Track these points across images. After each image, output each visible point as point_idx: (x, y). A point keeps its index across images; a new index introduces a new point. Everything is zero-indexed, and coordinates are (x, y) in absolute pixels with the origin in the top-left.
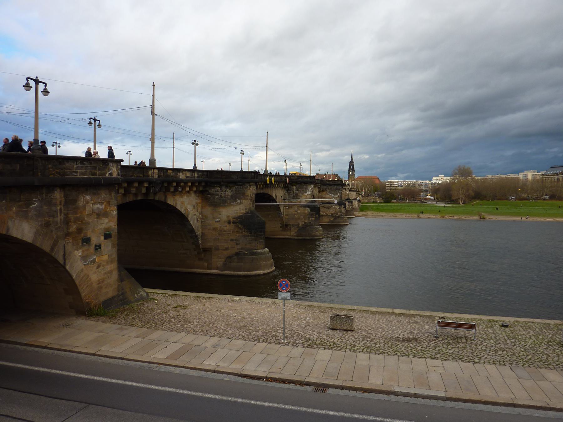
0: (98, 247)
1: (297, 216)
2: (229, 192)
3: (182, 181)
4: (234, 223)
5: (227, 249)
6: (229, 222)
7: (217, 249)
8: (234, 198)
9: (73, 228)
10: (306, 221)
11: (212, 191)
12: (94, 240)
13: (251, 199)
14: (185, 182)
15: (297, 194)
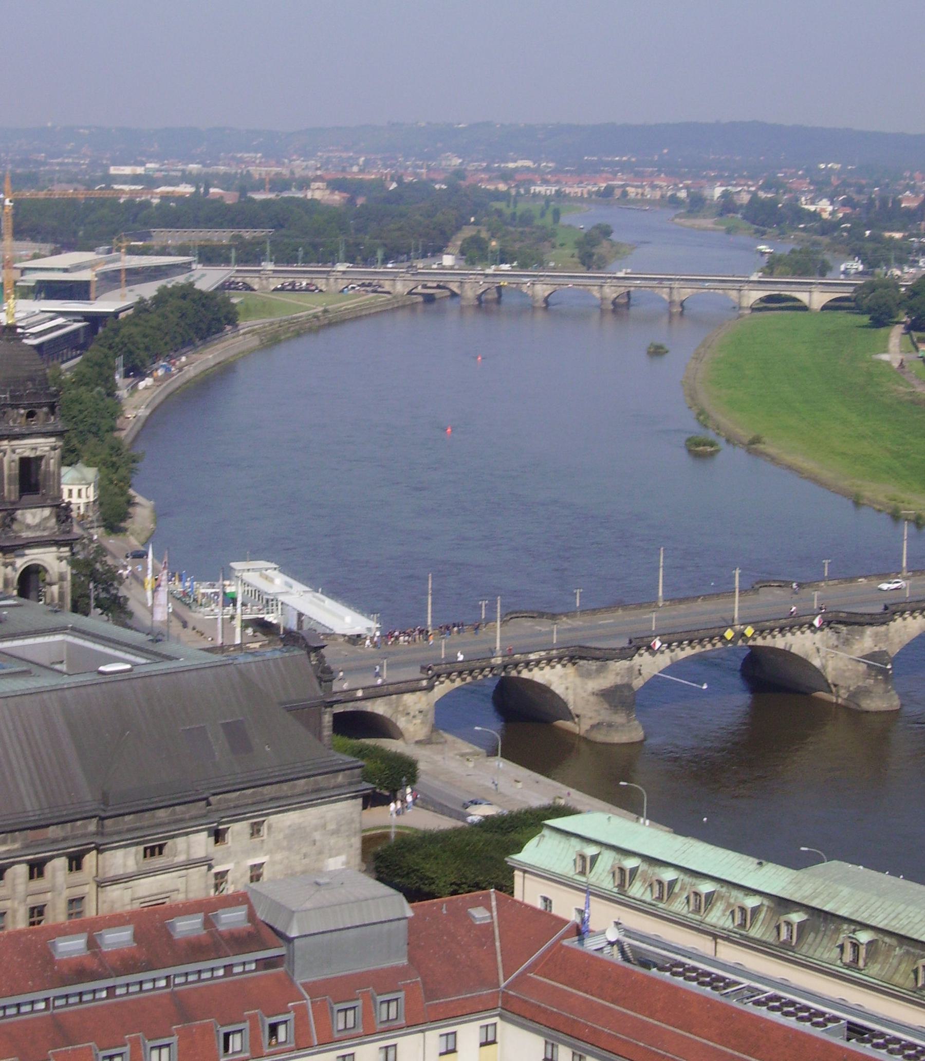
0: (414, 717)
1: (847, 674)
2: (593, 665)
3: (532, 661)
4: (597, 695)
5: (591, 718)
6: (593, 693)
7: (585, 716)
8: (599, 671)
9: (401, 708)
10: (860, 684)
11: (582, 662)
12: (412, 714)
13: (617, 674)
14: (538, 662)
15: (847, 640)
